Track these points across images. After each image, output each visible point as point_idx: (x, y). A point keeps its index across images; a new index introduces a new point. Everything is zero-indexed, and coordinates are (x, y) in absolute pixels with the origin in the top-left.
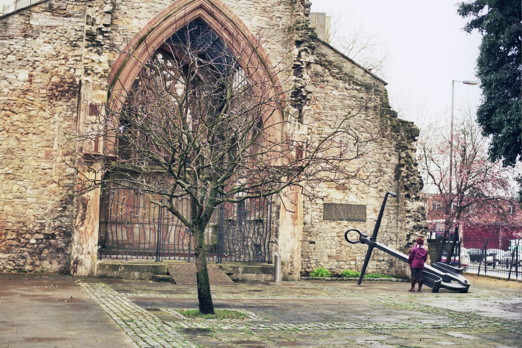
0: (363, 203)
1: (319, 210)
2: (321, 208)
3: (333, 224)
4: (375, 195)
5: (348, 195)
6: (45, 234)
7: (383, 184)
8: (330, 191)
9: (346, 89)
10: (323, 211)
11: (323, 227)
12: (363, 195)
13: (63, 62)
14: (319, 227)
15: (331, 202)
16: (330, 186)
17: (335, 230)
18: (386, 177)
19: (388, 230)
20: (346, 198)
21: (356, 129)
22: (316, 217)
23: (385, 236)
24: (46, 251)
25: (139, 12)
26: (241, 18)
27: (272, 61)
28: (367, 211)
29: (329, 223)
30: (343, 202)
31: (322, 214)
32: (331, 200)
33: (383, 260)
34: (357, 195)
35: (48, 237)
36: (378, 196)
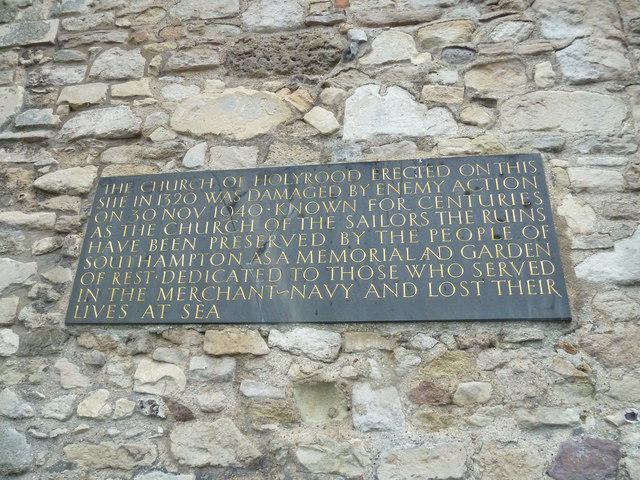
1: (46, 243)
5: (332, 92)
8: (175, 90)
12: (477, 81)
15: (168, 167)
16: (175, 61)
20: (322, 119)
31: (68, 275)
32: (176, 153)
34: (420, 81)
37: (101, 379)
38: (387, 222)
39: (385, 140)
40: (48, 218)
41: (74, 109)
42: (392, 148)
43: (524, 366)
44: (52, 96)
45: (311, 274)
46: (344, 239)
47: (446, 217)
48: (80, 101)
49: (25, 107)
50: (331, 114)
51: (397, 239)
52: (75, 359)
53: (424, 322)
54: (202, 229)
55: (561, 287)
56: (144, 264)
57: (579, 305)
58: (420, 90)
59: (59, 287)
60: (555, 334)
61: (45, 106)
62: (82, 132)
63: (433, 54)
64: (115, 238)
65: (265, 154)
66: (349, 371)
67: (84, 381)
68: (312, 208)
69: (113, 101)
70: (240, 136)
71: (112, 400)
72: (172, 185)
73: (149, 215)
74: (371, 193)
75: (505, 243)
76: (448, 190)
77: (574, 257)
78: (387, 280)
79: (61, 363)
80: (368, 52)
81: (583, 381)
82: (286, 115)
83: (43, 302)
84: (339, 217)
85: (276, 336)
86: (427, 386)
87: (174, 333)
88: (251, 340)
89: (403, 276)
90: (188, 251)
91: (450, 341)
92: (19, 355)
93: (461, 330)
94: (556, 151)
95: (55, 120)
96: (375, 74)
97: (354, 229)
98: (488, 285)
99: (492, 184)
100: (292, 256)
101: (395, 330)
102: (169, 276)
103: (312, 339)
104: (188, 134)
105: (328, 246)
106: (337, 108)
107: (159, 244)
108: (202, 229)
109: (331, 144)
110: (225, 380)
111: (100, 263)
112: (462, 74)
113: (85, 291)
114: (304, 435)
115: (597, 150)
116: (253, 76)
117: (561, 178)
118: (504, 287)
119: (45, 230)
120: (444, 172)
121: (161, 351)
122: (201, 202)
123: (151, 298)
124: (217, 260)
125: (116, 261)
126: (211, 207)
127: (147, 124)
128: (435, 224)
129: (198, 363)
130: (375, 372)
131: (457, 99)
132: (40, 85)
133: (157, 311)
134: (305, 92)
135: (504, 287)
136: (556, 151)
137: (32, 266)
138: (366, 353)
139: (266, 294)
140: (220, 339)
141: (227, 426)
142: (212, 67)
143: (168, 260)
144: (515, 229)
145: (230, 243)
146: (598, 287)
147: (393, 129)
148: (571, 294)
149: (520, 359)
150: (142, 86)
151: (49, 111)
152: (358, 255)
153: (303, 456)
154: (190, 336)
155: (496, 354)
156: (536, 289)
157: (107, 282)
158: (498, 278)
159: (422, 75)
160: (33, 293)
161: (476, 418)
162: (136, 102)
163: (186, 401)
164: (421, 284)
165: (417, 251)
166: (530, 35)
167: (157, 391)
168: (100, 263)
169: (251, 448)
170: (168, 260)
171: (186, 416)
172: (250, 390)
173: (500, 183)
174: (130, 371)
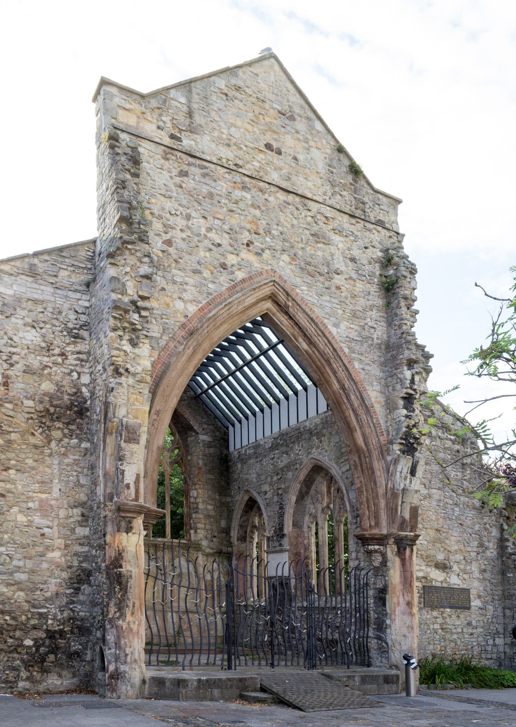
0: (465, 586)
3: (435, 613)
4: (478, 576)
6: (47, 631)
7: (486, 563)
8: (429, 570)
9: (439, 438)
11: (424, 617)
12: (465, 576)
13: (60, 360)
15: (430, 584)
16: (429, 564)
18: (488, 554)
19: (494, 620)
21: (453, 491)
23: (491, 628)
24: (52, 657)
25: (185, 290)
26: (326, 321)
27: (367, 388)
28: (471, 596)
29: (430, 612)
33: (491, 659)
35: (51, 635)
39: (455, 584)
81: (470, 616)
88: (443, 610)
141: (441, 619)
147: (456, 583)
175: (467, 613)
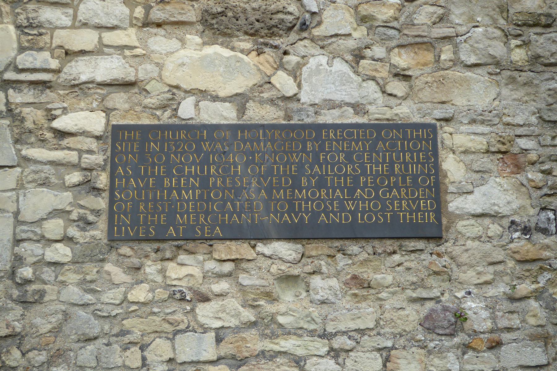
0: (406, 111)
1: (75, 177)
2: (88, 160)
3: (186, 270)
4: (498, 49)
5: (292, 59)
8: (160, 42)
10: (103, 180)
14: (74, 293)
15: (165, 117)
17: (205, 313)
20: (284, 82)
22: (54, 227)
28: (452, 167)
29: (151, 269)
30: (261, 113)
31: (102, 203)
32: (170, 104)
36: (519, 55)
37: (141, 278)
38: (332, 170)
39: (332, 105)
40: (73, 157)
41: (69, 54)
42: (336, 112)
43: (412, 265)
44: (47, 38)
45: (282, 207)
46: (304, 180)
47: (371, 167)
48: (76, 48)
49: (22, 49)
50: (291, 80)
51: (339, 183)
52: (117, 263)
53: (355, 239)
54: (202, 171)
55: (438, 219)
56: (162, 197)
57: (448, 229)
58: (358, 63)
59: (97, 212)
60: (431, 246)
61: (41, 49)
62: (83, 78)
63: (369, 29)
64: (137, 175)
65: (242, 110)
66: (309, 269)
67: (127, 278)
68: (281, 159)
69: (106, 50)
70: (222, 94)
71: (152, 290)
72: (174, 135)
73: (160, 159)
74: (322, 148)
75: (407, 188)
76: (373, 148)
77: (449, 197)
78: (332, 212)
79: (108, 267)
80: (319, 23)
82: (256, 79)
83: (85, 223)
84: (300, 166)
85: (261, 247)
86: (355, 277)
87: (190, 245)
88: (242, 249)
89: (342, 209)
90: (194, 188)
91: (370, 250)
92: (74, 262)
93: (376, 243)
94: (447, 120)
95: (54, 64)
96: (322, 43)
97: (311, 175)
98: (395, 217)
99: (403, 145)
100: (269, 192)
101: (337, 244)
102: (182, 206)
103: (285, 249)
104: (177, 87)
105: (293, 187)
106: (295, 73)
107: (171, 182)
108: (202, 171)
109: (294, 105)
110: (229, 275)
111: (127, 195)
112: (389, 50)
113: (119, 217)
114: (282, 308)
115: (473, 121)
116: (225, 35)
117: (448, 142)
118: (405, 216)
119: (75, 166)
120: (371, 134)
121: (183, 257)
122: (199, 151)
123: (171, 221)
124: (216, 195)
125: (139, 195)
126: (207, 154)
127: (141, 76)
128: (364, 173)
129: (211, 265)
130: (324, 269)
131: (383, 73)
132: (31, 26)
133: (177, 231)
134: (270, 55)
135: (405, 216)
136: (447, 120)
137: (68, 196)
138: (318, 257)
139: (253, 219)
140: (223, 249)
141: (233, 303)
142: (190, 24)
143: (179, 194)
144: (415, 178)
145: (224, 182)
146: (461, 217)
148: (444, 221)
149: (411, 262)
150: (128, 36)
151: (46, 54)
152: (313, 194)
153: (281, 320)
154: (203, 247)
155: (397, 258)
156: (423, 219)
157: (135, 211)
158: (401, 211)
159: (360, 49)
160: (74, 216)
161: (383, 295)
162: (127, 52)
163: (204, 289)
164: (353, 214)
165: (352, 192)
166: (441, 19)
167: (183, 283)
168: (127, 195)
169: (249, 315)
170: (179, 194)
171: (205, 299)
172: (245, 279)
173: (408, 144)
174: (162, 271)
175: (425, 258)
